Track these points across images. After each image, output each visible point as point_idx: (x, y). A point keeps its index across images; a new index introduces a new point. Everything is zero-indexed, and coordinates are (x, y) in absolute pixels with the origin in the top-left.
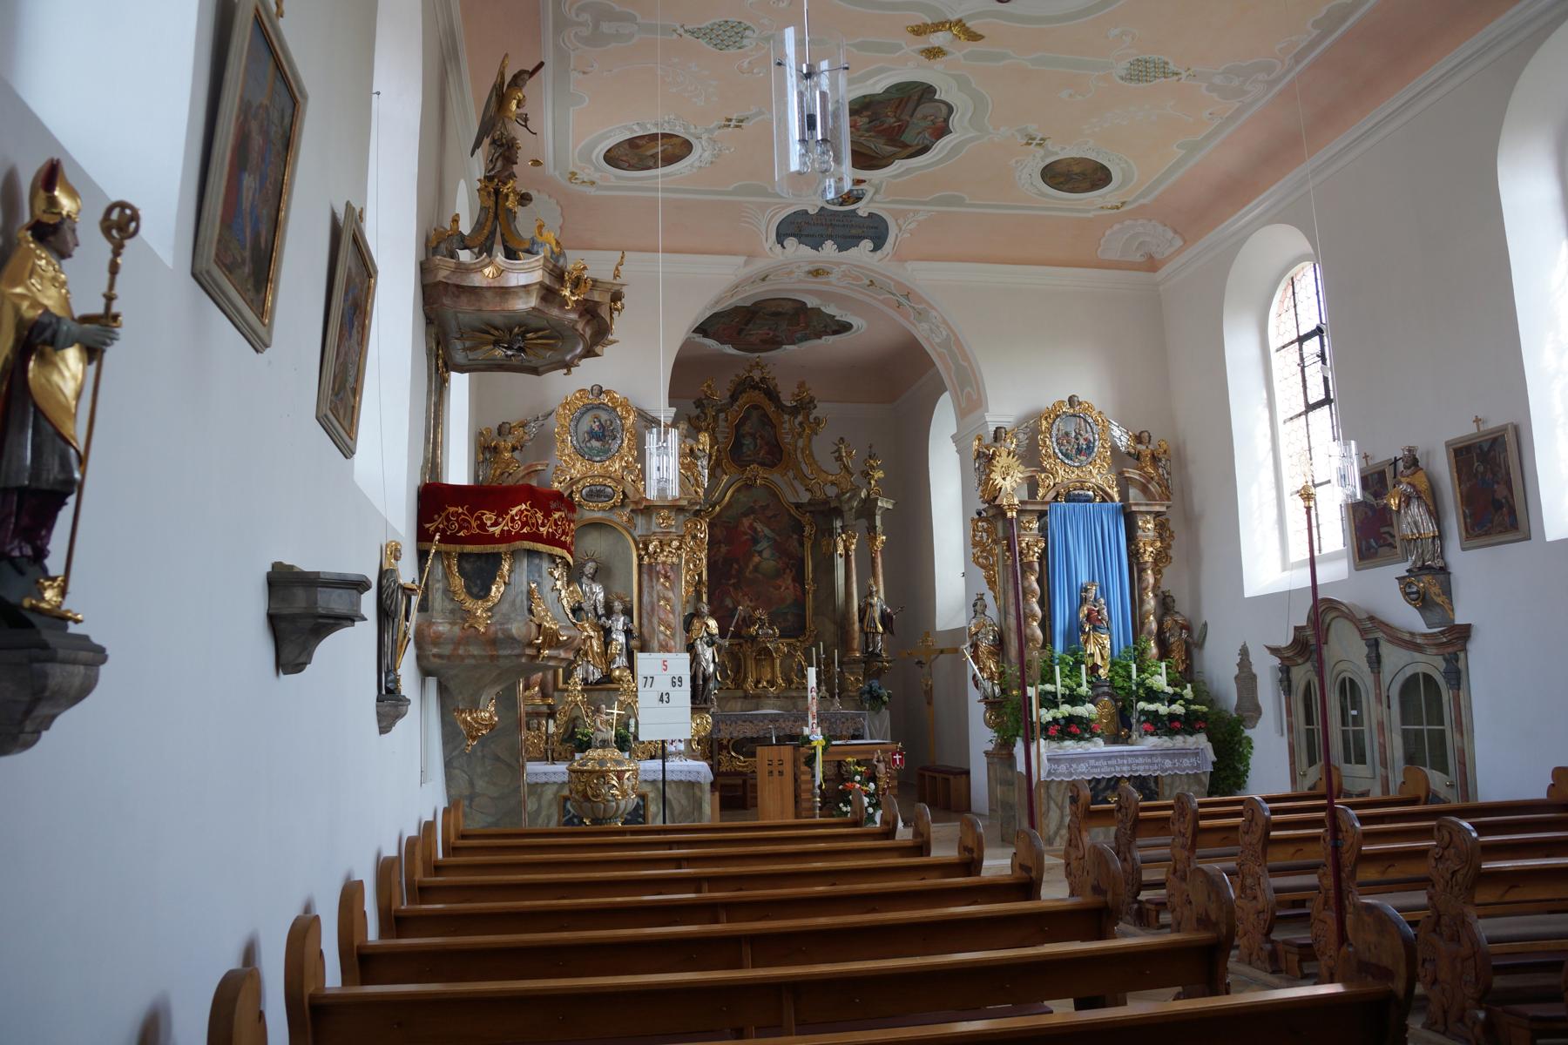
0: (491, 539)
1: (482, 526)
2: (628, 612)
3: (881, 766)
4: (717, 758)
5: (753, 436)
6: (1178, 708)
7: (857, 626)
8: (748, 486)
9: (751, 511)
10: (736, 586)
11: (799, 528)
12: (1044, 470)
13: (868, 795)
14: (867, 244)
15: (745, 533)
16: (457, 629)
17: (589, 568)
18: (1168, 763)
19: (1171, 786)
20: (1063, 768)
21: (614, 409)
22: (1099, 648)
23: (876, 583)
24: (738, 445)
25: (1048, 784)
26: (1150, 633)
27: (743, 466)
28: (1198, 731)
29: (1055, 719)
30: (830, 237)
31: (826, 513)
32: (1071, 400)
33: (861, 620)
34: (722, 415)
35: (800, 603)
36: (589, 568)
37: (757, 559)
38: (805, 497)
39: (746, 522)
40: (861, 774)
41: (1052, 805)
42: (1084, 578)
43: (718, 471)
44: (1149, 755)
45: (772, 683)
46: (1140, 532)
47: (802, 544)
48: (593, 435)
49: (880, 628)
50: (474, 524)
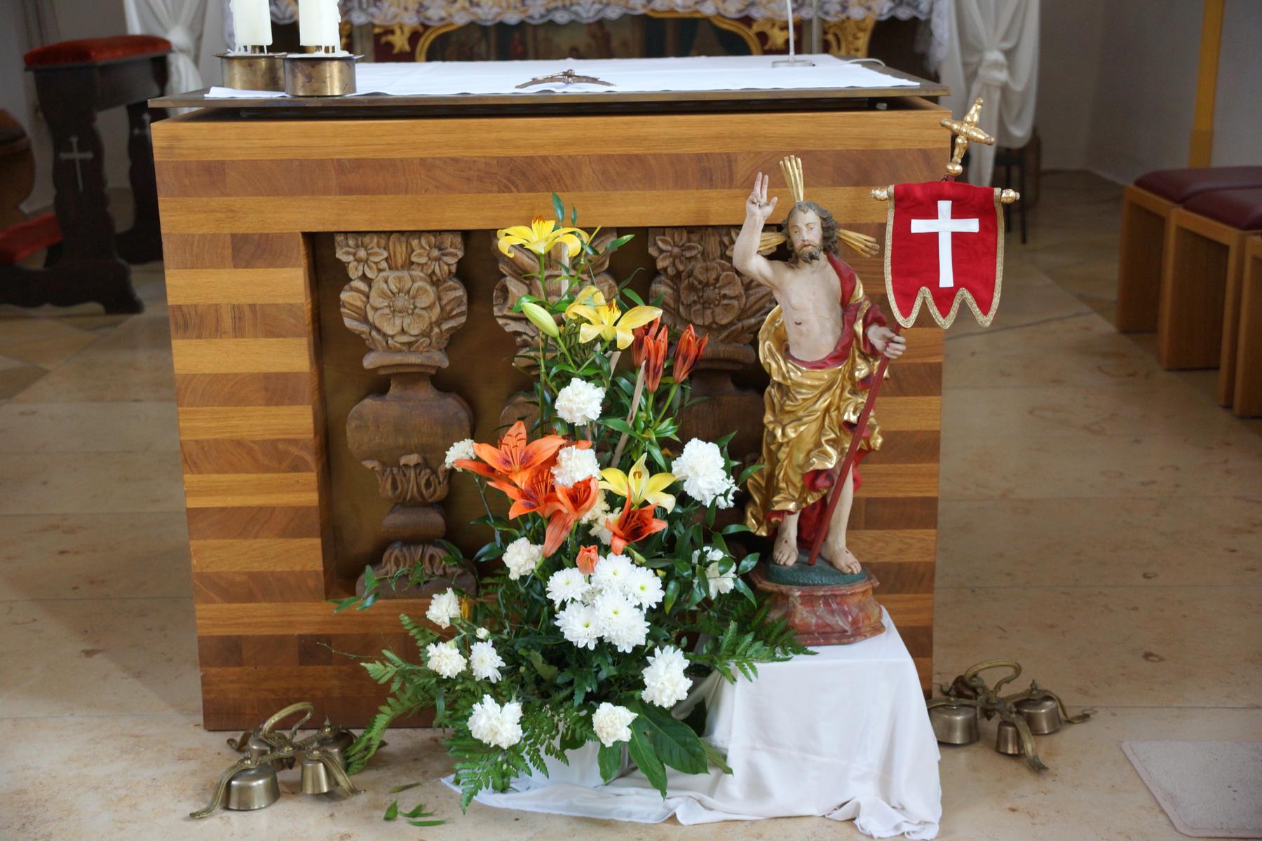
3: (807, 304)
13: (661, 541)
40: (614, 371)
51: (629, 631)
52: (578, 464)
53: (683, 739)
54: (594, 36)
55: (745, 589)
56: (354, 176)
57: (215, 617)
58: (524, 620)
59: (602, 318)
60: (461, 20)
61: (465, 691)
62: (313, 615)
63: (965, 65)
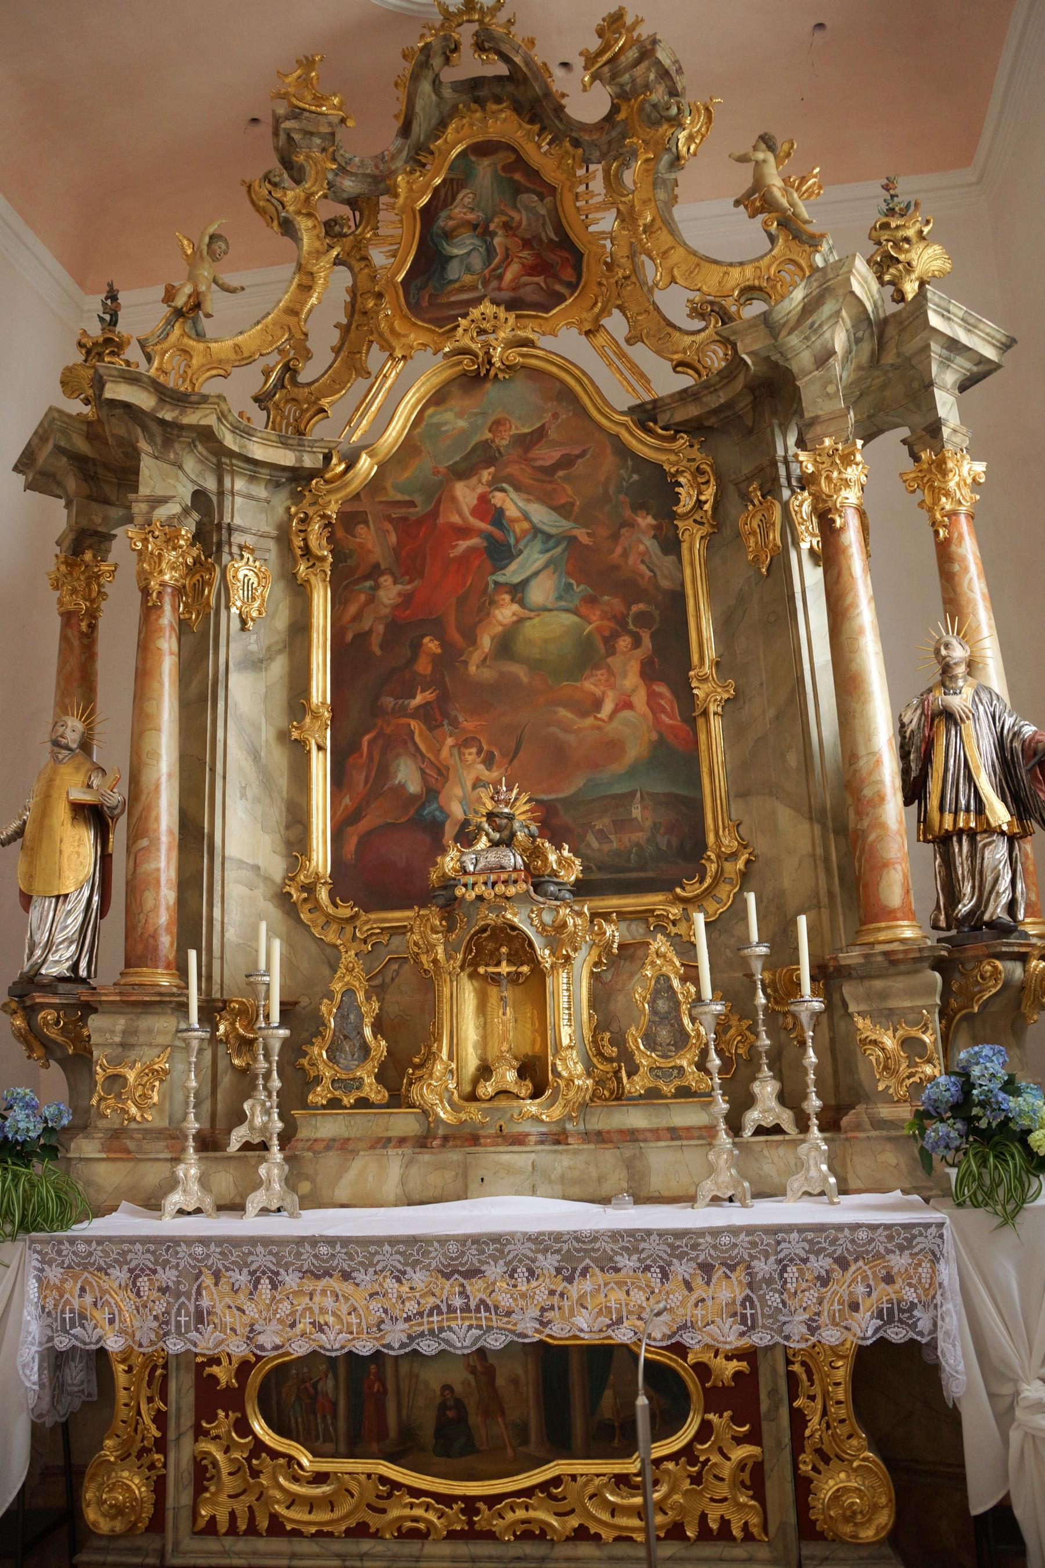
5: (482, 231)
7: (893, 810)
8: (473, 378)
10: (433, 717)
11: (657, 490)
15: (464, 532)
23: (967, 636)
24: (430, 261)
31: (747, 406)
33: (914, 790)
35: (677, 757)
37: (506, 612)
38: (666, 382)
39: (466, 494)
45: (535, 1073)
47: (671, 545)
49: (1000, 813)
54: (473, 1371)
60: (299, 1349)
63: (991, 1396)
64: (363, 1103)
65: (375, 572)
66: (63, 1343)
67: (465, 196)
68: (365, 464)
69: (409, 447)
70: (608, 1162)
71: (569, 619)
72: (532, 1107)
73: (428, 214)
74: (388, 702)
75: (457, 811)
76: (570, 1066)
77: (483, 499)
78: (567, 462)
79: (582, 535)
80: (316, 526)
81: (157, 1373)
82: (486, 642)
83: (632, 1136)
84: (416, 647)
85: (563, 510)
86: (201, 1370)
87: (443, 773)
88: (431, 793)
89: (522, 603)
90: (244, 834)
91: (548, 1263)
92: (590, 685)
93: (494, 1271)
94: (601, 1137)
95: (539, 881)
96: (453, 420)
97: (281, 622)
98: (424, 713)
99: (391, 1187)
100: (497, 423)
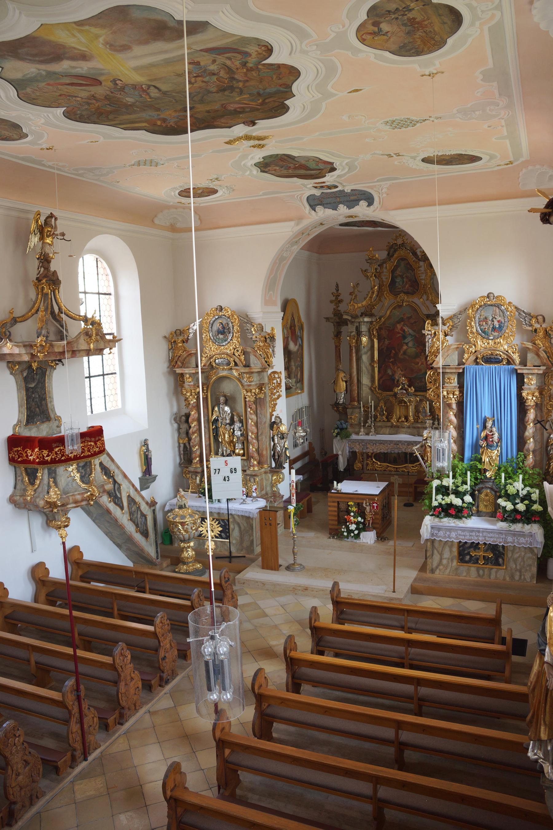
0: (29, 462)
1: (27, 456)
2: (241, 421)
3: (368, 509)
4: (365, 462)
6: (521, 507)
9: (401, 320)
12: (469, 342)
13: (357, 523)
14: (363, 203)
15: (399, 333)
16: (21, 499)
17: (222, 399)
18: (510, 539)
19: (513, 551)
20: (441, 533)
21: (229, 318)
22: (491, 458)
25: (433, 541)
26: (528, 450)
27: (396, 294)
28: (535, 522)
29: (440, 504)
30: (341, 203)
32: (488, 296)
34: (385, 265)
36: (222, 399)
37: (405, 347)
39: (399, 326)
41: (435, 552)
42: (486, 412)
43: (382, 299)
44: (500, 532)
45: (407, 418)
46: (526, 386)
48: (219, 332)
50: (24, 455)
51: (354, 529)
52: (352, 518)
53: (357, 536)
55: (363, 528)
56: (340, 498)
57: (331, 527)
58: (348, 527)
59: (354, 509)
60: (378, 452)
61: (344, 532)
62: (336, 527)
64: (384, 421)
65: (384, 338)
66: (351, 450)
67: (399, 269)
68: (383, 319)
69: (390, 317)
70: (415, 431)
71: (414, 349)
72: (406, 423)
73: (393, 272)
74: (387, 360)
75: (397, 378)
76: (411, 418)
77: (402, 328)
78: (415, 322)
79: (417, 335)
80: (375, 330)
81: (362, 454)
82: (402, 352)
83: (418, 428)
84: (391, 351)
85: (414, 331)
86: (367, 454)
87: (395, 372)
88: (393, 375)
89: (407, 346)
90: (366, 381)
91: (406, 444)
92: (417, 360)
93: (400, 444)
94: (414, 428)
95: (408, 394)
96: (397, 312)
97: (369, 346)
98: (392, 362)
99: (387, 432)
100: (404, 314)
